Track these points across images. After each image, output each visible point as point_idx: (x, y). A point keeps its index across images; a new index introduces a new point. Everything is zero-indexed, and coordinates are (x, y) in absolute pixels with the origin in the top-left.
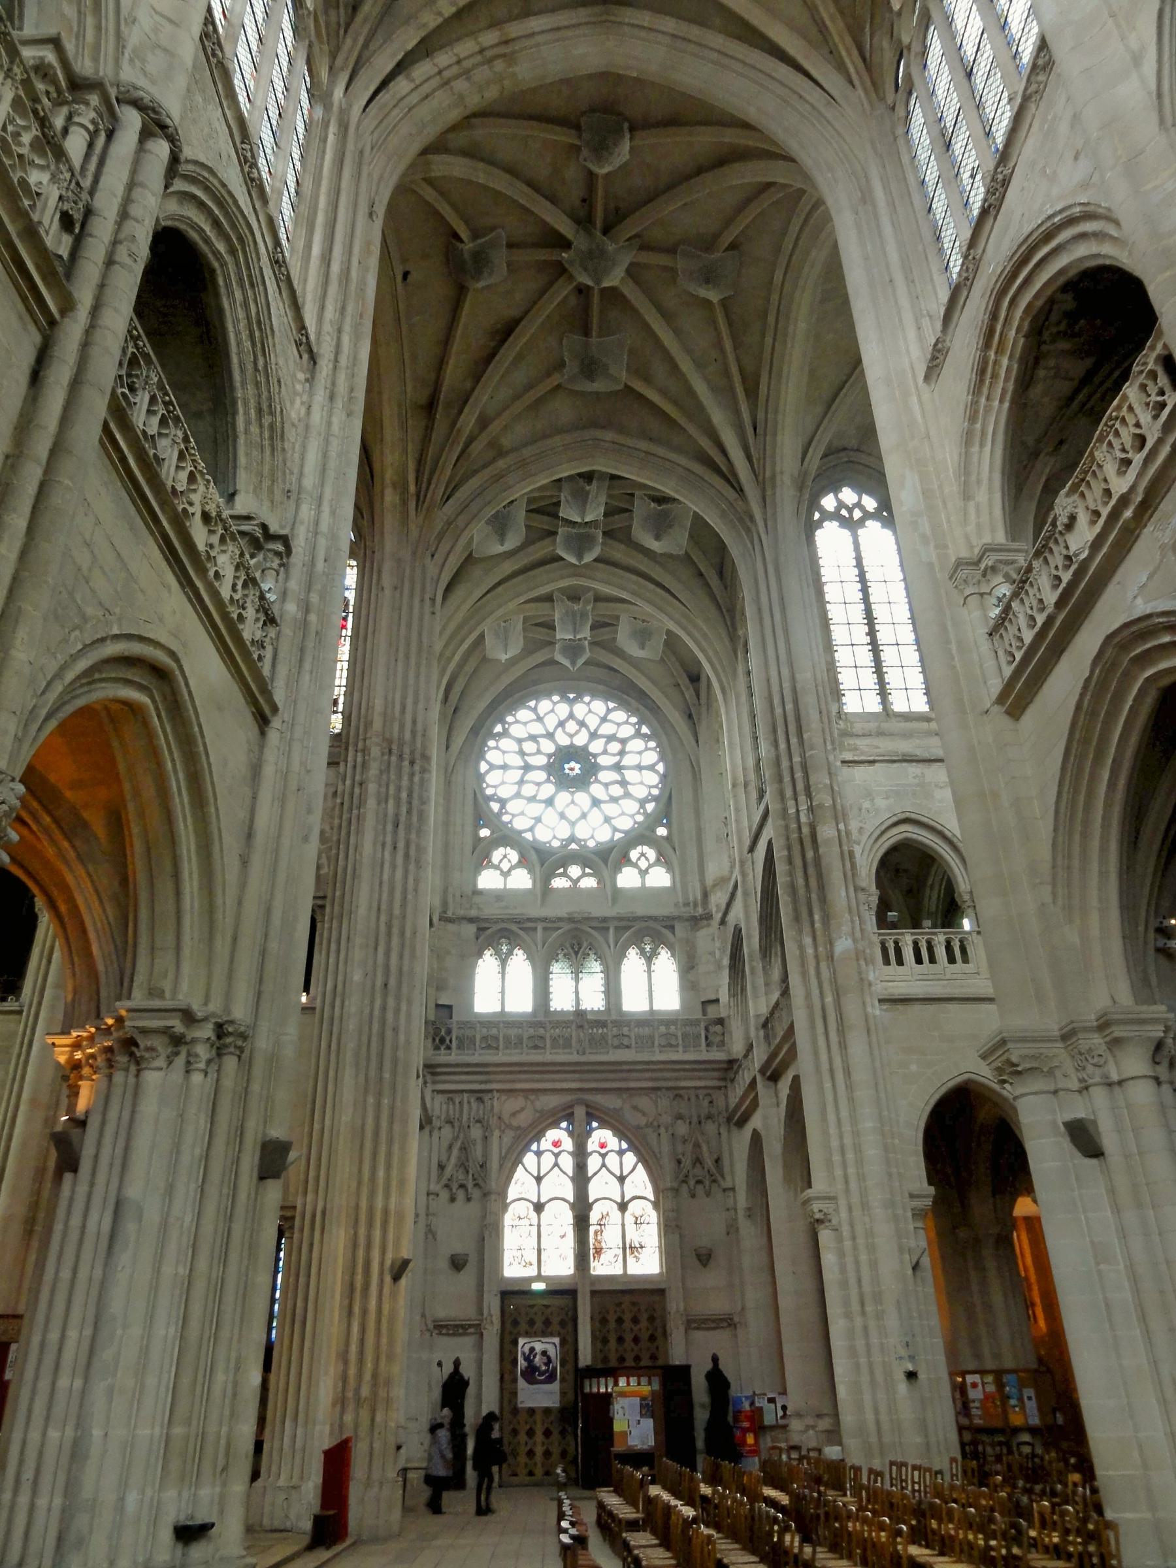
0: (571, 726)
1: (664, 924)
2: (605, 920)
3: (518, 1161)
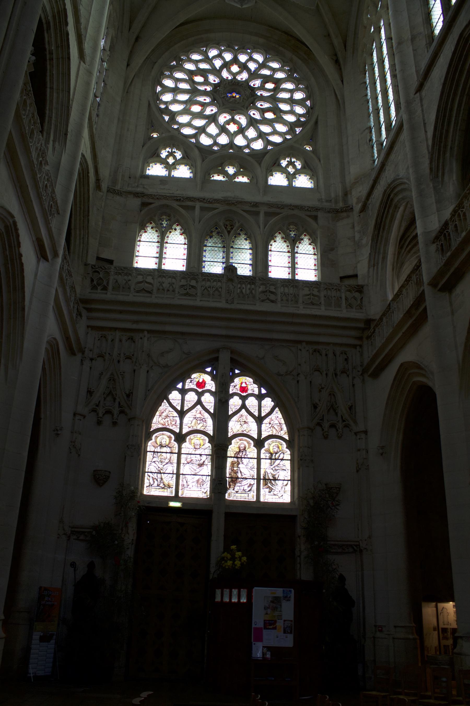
0: (235, 69)
1: (309, 213)
2: (256, 205)
3: (164, 396)
